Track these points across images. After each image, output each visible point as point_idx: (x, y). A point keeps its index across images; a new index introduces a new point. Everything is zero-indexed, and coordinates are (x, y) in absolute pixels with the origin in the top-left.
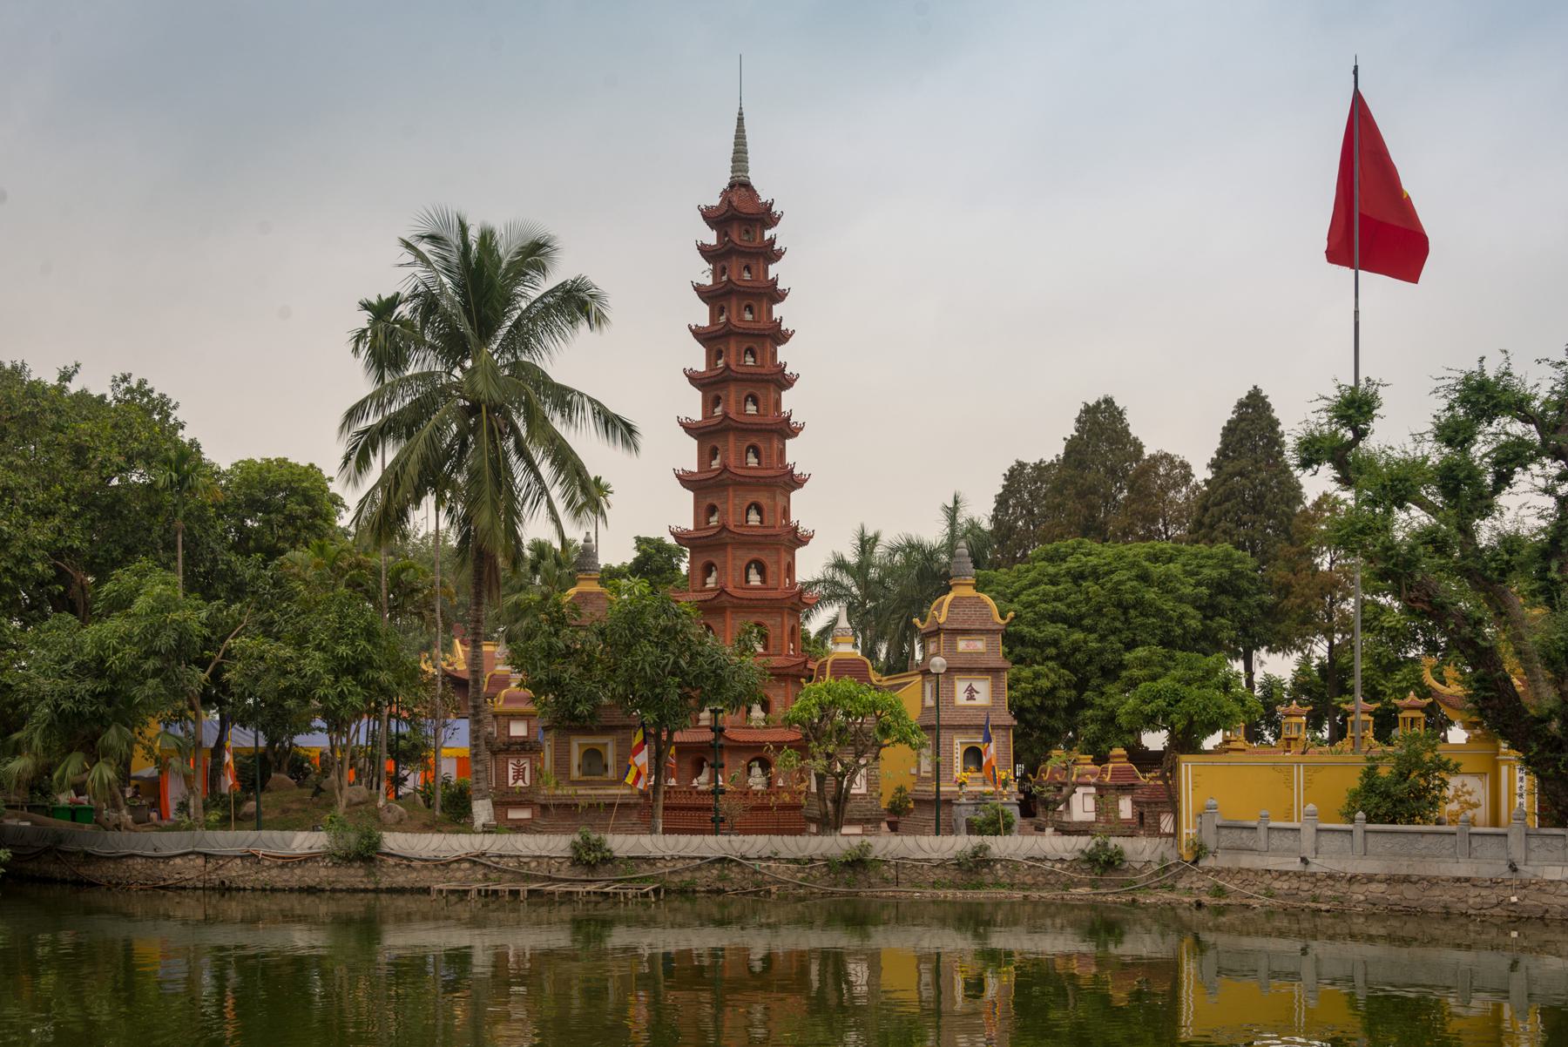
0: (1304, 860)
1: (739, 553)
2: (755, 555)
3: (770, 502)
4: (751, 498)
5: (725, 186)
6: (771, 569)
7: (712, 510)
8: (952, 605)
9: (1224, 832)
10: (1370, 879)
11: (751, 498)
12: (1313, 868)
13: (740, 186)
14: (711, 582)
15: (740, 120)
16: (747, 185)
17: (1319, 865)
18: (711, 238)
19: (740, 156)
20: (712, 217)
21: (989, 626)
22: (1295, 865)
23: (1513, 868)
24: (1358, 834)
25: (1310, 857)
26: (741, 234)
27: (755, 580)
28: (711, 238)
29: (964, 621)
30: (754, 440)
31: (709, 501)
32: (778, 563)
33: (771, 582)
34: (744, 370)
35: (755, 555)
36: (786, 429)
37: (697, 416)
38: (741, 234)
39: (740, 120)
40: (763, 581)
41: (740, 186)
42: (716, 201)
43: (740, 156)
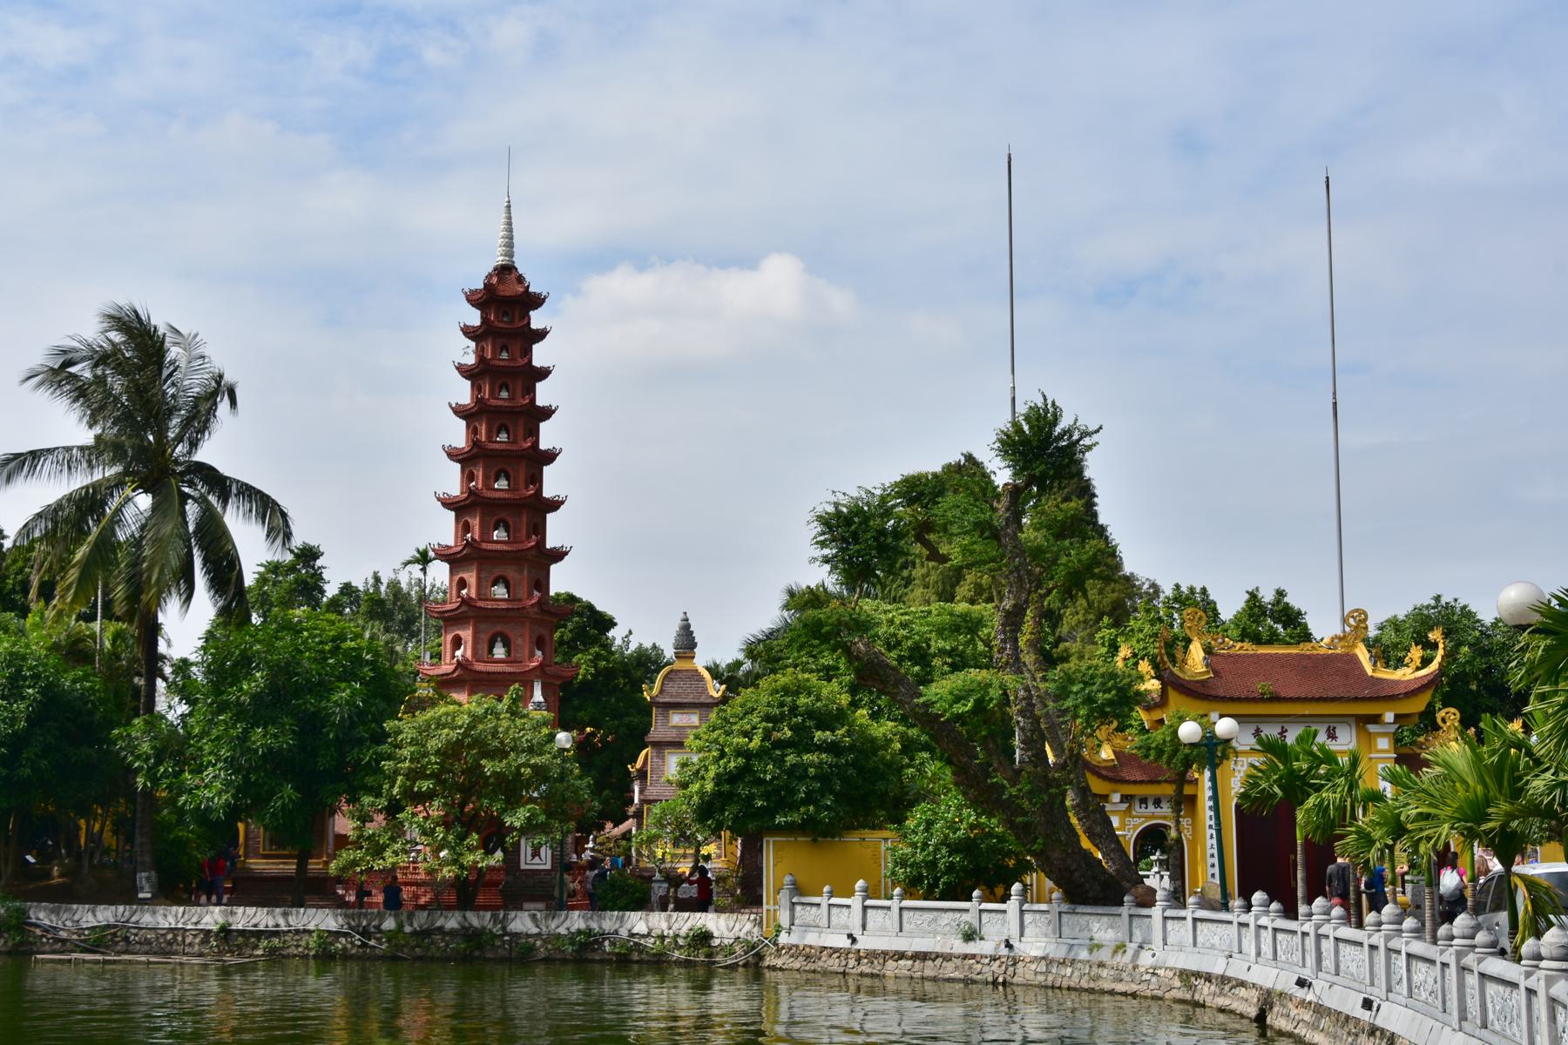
0: (850, 936)
1: (482, 626)
2: (499, 628)
3: (516, 575)
4: (497, 572)
8: (666, 677)
9: (798, 908)
10: (901, 955)
11: (497, 572)
12: (857, 946)
17: (865, 943)
18: (474, 318)
20: (474, 299)
21: (703, 700)
22: (844, 943)
23: (1009, 946)
24: (895, 910)
25: (857, 933)
26: (506, 314)
27: (499, 652)
28: (474, 318)
29: (678, 695)
30: (503, 515)
35: (499, 628)
38: (506, 314)
40: (508, 653)
41: (506, 270)
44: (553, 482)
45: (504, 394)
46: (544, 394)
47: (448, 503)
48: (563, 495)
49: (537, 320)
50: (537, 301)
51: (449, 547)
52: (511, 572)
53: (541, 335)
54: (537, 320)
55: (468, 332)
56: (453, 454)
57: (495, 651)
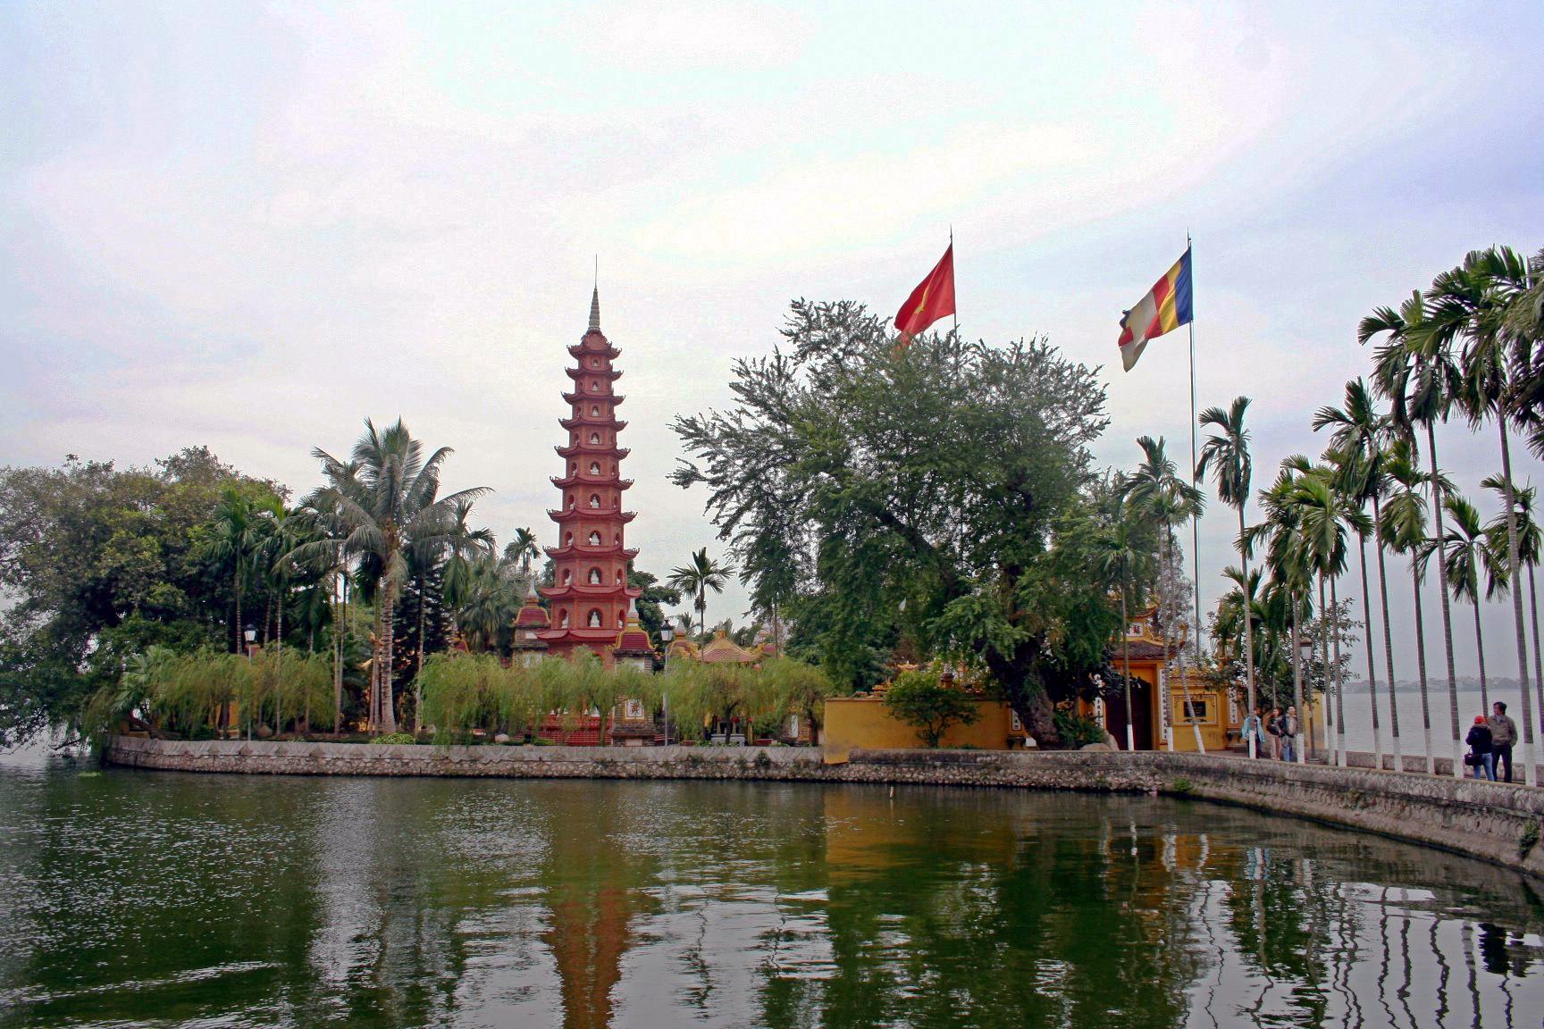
2: (595, 564)
4: (594, 528)
6: (606, 574)
7: (569, 536)
11: (594, 528)
13: (594, 333)
14: (568, 581)
15: (596, 293)
16: (598, 333)
18: (574, 364)
20: (574, 352)
26: (594, 360)
27: (595, 580)
28: (574, 364)
30: (596, 491)
31: (568, 530)
33: (606, 582)
35: (595, 564)
37: (563, 475)
39: (596, 293)
41: (594, 333)
42: (579, 342)
44: (625, 470)
46: (620, 413)
47: (558, 483)
49: (616, 364)
50: (615, 354)
52: (601, 528)
55: (570, 373)
56: (561, 452)
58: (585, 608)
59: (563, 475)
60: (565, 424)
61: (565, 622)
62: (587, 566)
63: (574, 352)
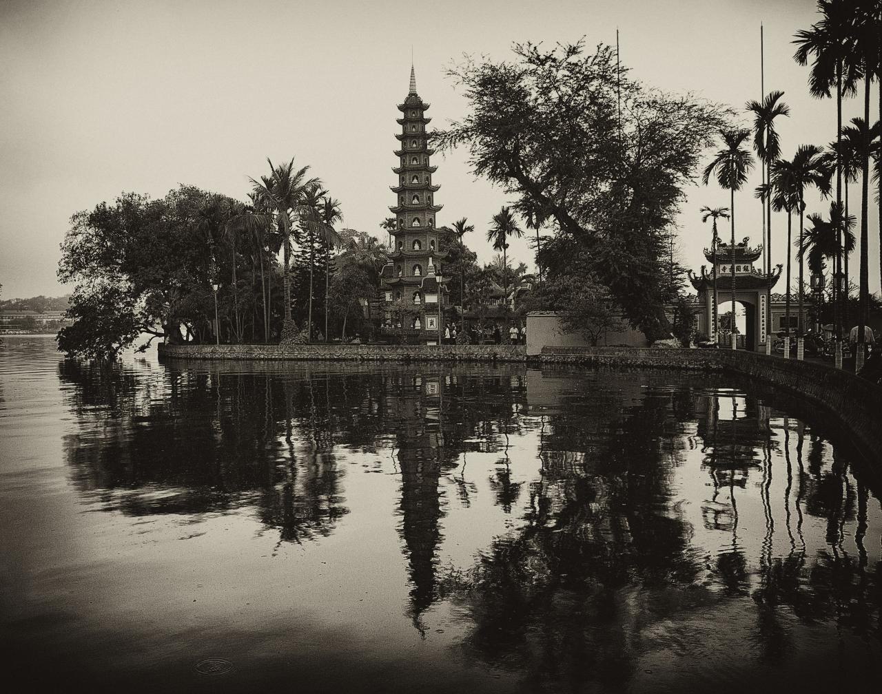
5: (407, 95)
6: (423, 243)
13: (413, 95)
15: (413, 70)
16: (416, 95)
18: (401, 115)
19: (412, 84)
20: (401, 108)
27: (417, 247)
28: (401, 115)
32: (426, 241)
34: (413, 166)
36: (430, 189)
37: (397, 185)
39: (413, 70)
40: (420, 247)
41: (413, 95)
43: (412, 84)
45: (414, 145)
48: (439, 185)
49: (426, 114)
50: (426, 107)
51: (395, 208)
53: (428, 121)
54: (426, 114)
55: (399, 122)
57: (415, 247)
58: (411, 265)
59: (397, 185)
60: (397, 153)
61: (400, 273)
62: (412, 239)
63: (401, 108)
